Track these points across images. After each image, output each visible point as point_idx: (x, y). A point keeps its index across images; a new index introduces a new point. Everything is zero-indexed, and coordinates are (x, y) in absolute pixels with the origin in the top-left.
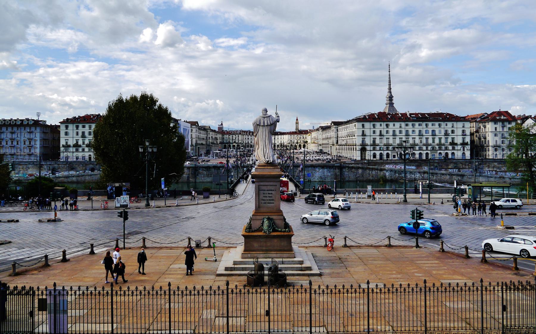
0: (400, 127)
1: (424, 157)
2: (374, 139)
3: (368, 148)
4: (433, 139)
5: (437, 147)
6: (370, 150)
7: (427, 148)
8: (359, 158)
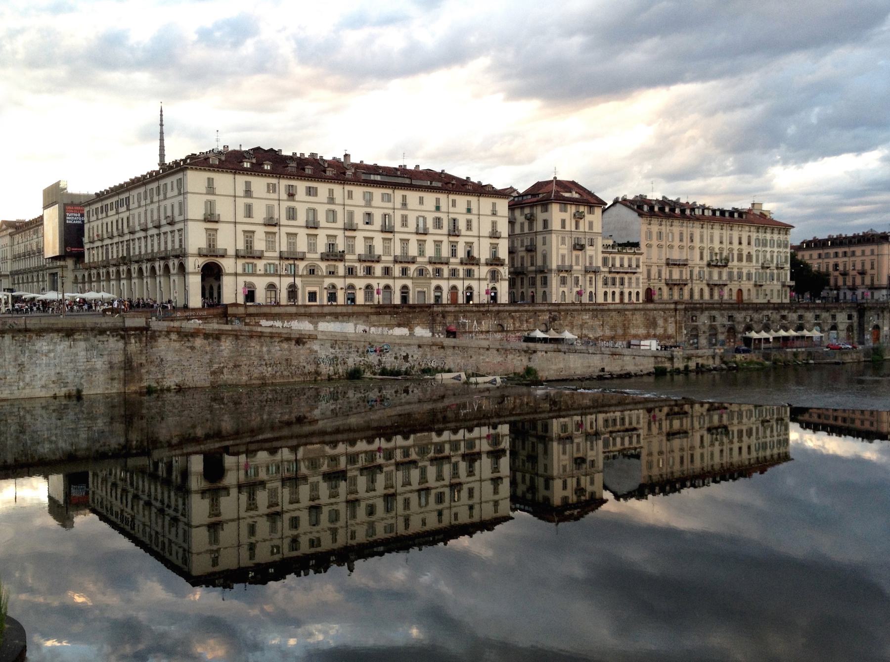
0: (331, 200)
1: (397, 301)
2: (249, 234)
3: (227, 264)
4: (421, 243)
5: (430, 268)
6: (236, 274)
7: (404, 271)
8: (196, 301)
